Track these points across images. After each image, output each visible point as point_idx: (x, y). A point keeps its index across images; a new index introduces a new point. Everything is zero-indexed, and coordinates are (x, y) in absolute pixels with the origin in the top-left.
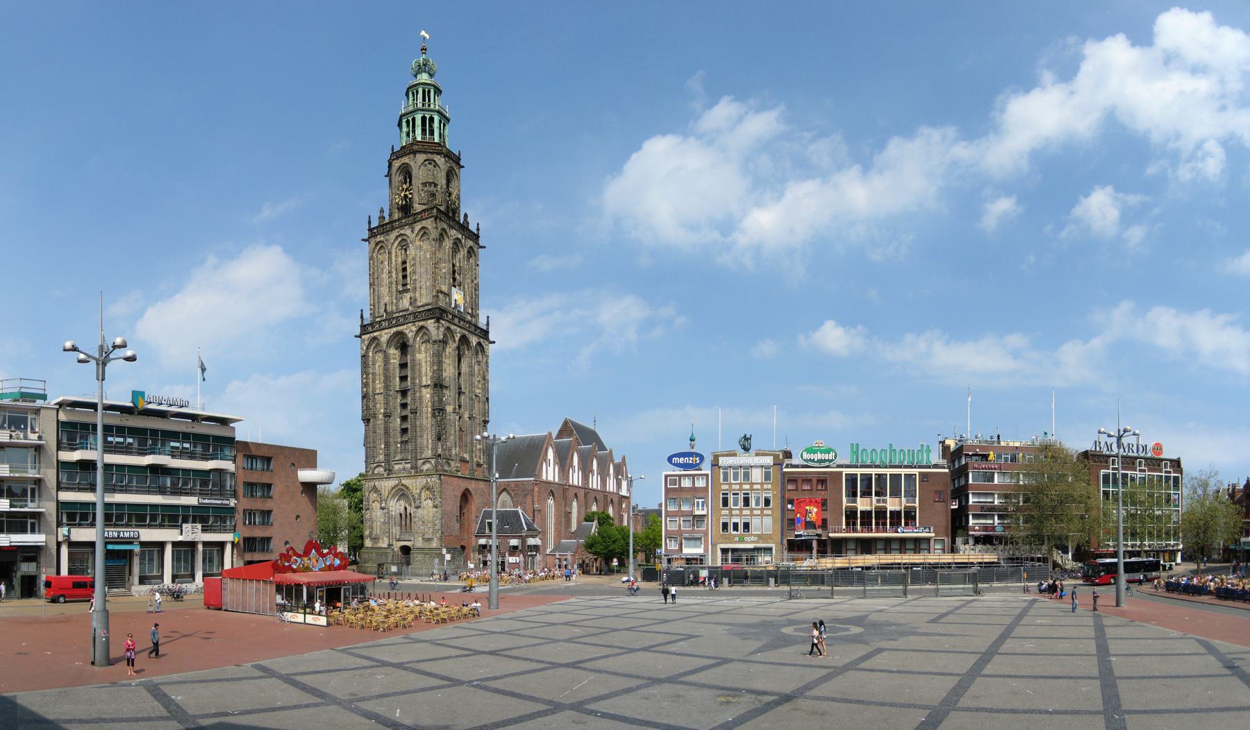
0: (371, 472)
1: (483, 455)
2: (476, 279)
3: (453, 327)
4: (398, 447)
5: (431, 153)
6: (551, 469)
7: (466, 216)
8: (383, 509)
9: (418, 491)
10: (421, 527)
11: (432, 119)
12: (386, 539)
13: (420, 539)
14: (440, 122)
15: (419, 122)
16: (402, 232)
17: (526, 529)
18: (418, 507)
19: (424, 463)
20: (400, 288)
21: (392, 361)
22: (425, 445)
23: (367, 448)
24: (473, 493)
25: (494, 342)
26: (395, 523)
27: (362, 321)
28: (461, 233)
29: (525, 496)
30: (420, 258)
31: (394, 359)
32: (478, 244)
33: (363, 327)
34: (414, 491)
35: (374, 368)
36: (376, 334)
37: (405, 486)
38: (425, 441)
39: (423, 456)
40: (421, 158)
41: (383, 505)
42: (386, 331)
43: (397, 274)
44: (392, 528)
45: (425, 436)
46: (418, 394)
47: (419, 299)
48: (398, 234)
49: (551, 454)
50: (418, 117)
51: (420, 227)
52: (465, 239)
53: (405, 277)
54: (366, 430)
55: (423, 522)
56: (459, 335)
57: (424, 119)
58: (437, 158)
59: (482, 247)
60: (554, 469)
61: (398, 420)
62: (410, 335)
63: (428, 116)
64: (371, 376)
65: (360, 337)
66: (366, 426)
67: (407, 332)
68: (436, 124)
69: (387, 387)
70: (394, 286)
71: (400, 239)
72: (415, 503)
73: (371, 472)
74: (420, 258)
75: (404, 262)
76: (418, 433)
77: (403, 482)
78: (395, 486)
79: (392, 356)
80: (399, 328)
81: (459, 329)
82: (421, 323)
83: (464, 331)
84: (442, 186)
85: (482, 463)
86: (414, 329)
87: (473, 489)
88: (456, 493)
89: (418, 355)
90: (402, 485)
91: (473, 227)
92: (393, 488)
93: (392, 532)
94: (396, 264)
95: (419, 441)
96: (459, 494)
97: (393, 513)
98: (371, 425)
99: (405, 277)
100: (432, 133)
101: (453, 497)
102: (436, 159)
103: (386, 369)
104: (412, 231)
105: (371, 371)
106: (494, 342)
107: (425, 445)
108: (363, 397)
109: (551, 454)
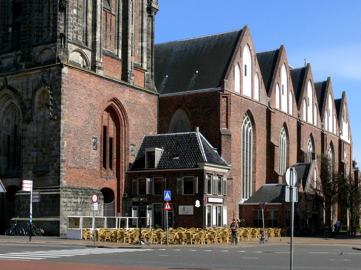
1: (148, 57)
4: (8, 34)
6: (247, 80)
9: (30, 95)
10: (32, 154)
18: (28, 121)
19: (41, 52)
22: (45, 23)
24: (127, 108)
34: (25, 97)
38: (46, 18)
39: (40, 42)
45: (46, 11)
60: (252, 80)
72: (24, 114)
77: (10, 83)
87: (128, 103)
88: (93, 101)
90: (10, 88)
101: (88, 108)
107: (45, 23)
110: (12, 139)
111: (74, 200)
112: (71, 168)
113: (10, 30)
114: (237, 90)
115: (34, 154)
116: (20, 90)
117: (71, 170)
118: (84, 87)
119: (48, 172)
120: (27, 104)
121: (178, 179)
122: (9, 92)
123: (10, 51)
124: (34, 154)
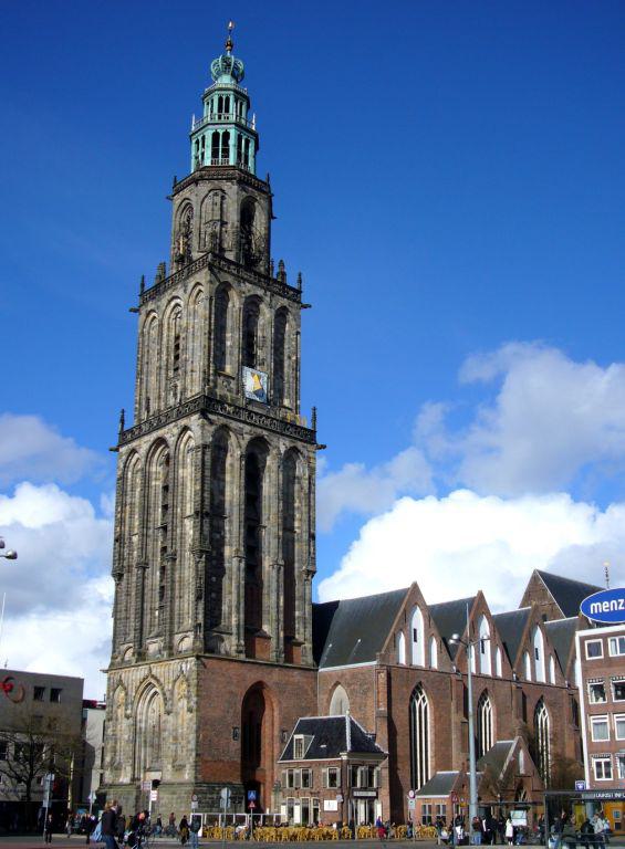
0: (119, 659)
3: (234, 425)
5: (217, 179)
7: (282, 264)
8: (128, 717)
11: (226, 135)
12: (129, 769)
13: (170, 766)
14: (239, 138)
15: (209, 142)
16: (174, 294)
17: (349, 748)
18: (168, 713)
19: (182, 640)
20: (171, 374)
21: (153, 483)
22: (186, 611)
23: (116, 620)
25: (324, 447)
26: (145, 741)
27: (123, 426)
28: (262, 287)
29: (365, 693)
30: (193, 327)
31: (156, 479)
32: (299, 302)
33: (123, 434)
34: (166, 687)
35: (133, 497)
36: (134, 444)
37: (155, 678)
38: (186, 605)
40: (204, 188)
41: (129, 712)
42: (146, 438)
43: (168, 355)
44: (140, 751)
45: (186, 596)
46: (178, 531)
47: (189, 387)
48: (169, 298)
49: (539, 640)
50: (209, 134)
51: (193, 284)
52: (272, 295)
53: (177, 357)
54: (117, 592)
55: (175, 738)
56: (247, 437)
57: (215, 136)
58: (226, 186)
59: (305, 307)
61: (158, 573)
62: (171, 440)
63: (221, 132)
64: (128, 507)
65: (117, 450)
66: (117, 585)
67: (167, 436)
68: (232, 142)
69: (145, 524)
70: (163, 372)
71: (173, 304)
73: (119, 659)
74: (193, 327)
75: (177, 338)
76: (177, 592)
77: (154, 672)
78: (144, 679)
79: (154, 476)
80: (159, 433)
81: (247, 428)
82: (183, 422)
83: (259, 431)
84: (233, 224)
85: (302, 640)
86: (176, 431)
88: (233, 688)
89: (181, 471)
90: (153, 676)
91: (291, 281)
92: (141, 683)
93: (140, 758)
94: (168, 340)
95: (177, 604)
96: (241, 692)
97: (143, 725)
98: (124, 583)
99: (177, 357)
100: (226, 152)
101: (228, 696)
102: (225, 188)
103: (145, 496)
104: (185, 291)
105: (129, 501)
106: (324, 447)
107: (186, 611)
108: (116, 540)
109: (539, 640)
110: (157, 729)
111: (209, 796)
112: (206, 762)
113: (157, 613)
114: (403, 660)
115: (173, 747)
116: (162, 680)
117: (208, 764)
118: (223, 675)
119: (185, 766)
120: (168, 694)
121: (323, 770)
122: (153, 681)
123: (157, 636)
124: (173, 747)
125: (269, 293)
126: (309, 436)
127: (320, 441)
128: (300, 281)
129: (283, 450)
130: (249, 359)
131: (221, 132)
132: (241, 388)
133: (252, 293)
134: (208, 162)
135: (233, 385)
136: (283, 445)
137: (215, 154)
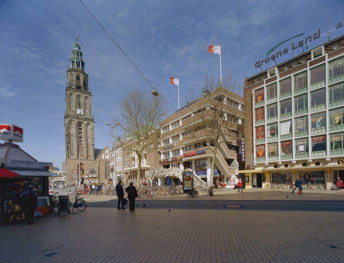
2: (90, 105)
3: (73, 120)
11: (74, 61)
14: (77, 61)
56: (77, 122)
58: (73, 72)
59: (92, 96)
63: (73, 60)
68: (75, 62)
81: (77, 120)
102: (72, 73)
125: (82, 94)
126: (92, 120)
127: (95, 121)
128: (91, 91)
129: (86, 123)
130: (80, 107)
131: (73, 60)
132: (76, 112)
133: (78, 94)
134: (71, 68)
135: (74, 112)
136: (86, 123)
137: (72, 66)
